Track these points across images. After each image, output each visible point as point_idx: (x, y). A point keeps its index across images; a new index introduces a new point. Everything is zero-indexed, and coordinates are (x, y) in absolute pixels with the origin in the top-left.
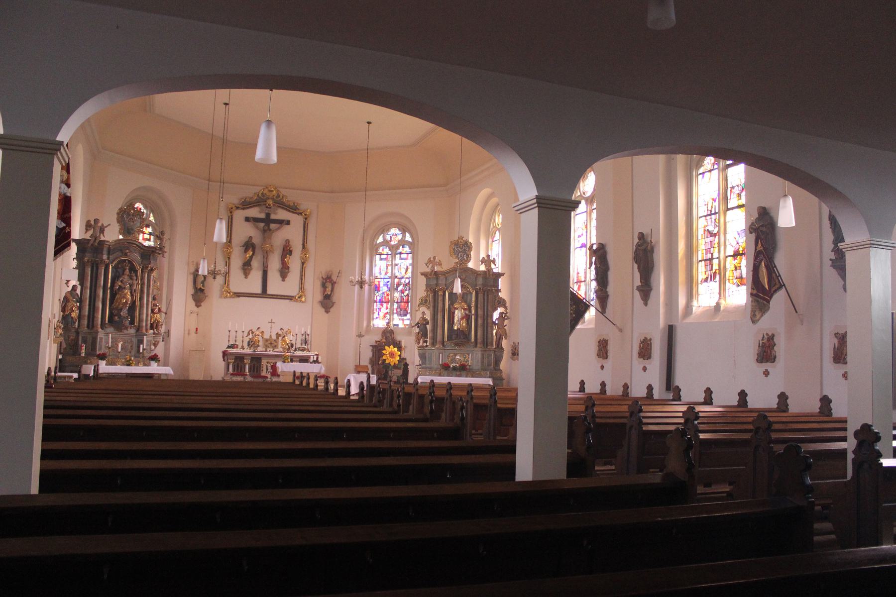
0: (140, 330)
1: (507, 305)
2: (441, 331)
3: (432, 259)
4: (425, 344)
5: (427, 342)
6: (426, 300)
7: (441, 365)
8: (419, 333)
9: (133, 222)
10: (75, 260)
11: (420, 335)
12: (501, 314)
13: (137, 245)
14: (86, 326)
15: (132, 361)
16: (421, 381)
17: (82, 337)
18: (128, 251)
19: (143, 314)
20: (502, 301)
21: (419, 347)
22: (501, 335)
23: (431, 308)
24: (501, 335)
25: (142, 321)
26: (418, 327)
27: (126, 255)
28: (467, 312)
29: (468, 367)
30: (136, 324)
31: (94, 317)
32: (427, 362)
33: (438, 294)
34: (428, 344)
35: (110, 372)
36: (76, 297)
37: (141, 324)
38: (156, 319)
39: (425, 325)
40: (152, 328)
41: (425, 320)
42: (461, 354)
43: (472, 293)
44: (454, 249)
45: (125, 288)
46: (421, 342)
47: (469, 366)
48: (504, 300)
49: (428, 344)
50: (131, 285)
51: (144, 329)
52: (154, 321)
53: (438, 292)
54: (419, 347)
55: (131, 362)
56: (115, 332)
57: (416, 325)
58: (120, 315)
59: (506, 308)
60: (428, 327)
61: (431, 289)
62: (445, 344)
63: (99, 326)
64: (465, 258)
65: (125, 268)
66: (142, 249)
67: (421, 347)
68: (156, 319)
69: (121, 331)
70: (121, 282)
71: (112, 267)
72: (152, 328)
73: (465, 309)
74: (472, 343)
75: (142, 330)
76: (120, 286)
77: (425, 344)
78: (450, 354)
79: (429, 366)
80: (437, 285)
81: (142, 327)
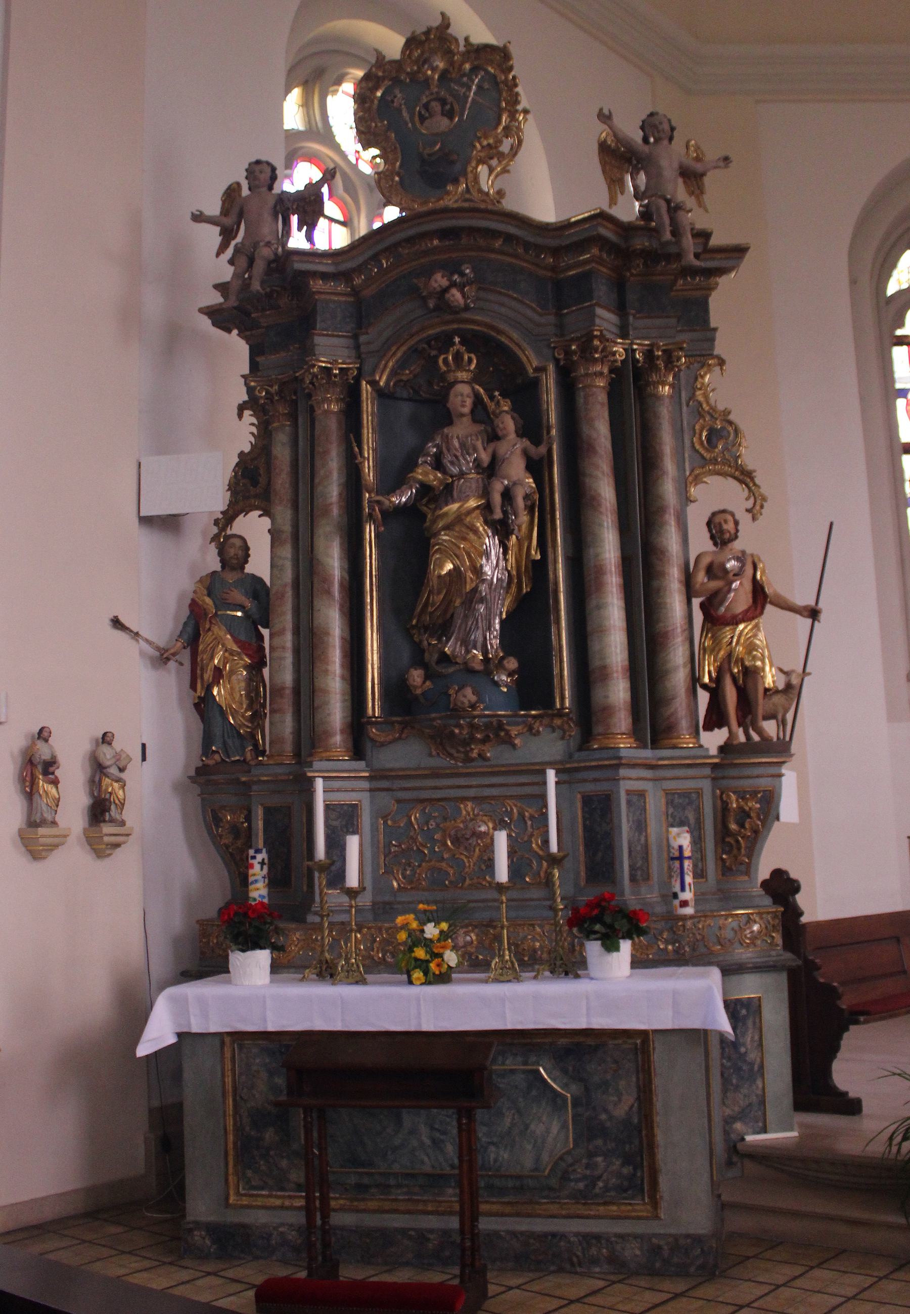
0: (598, 729)
9: (450, 115)
10: (247, 413)
13: (509, 238)
14: (288, 747)
15: (428, 944)
17: (268, 811)
18: (439, 280)
19: (602, 631)
25: (604, 674)
27: (443, 305)
30: (566, 697)
31: (313, 691)
35: (271, 1028)
36: (238, 596)
37: (598, 695)
38: (730, 655)
40: (716, 718)
45: (448, 492)
50: (491, 470)
51: (622, 721)
52: (719, 670)
55: (420, 953)
56: (440, 762)
58: (445, 659)
63: (338, 739)
65: (451, 377)
66: (539, 248)
68: (730, 655)
69: (468, 760)
70: (438, 464)
71: (381, 394)
72: (716, 718)
75: (607, 734)
76: (425, 489)
81: (608, 710)
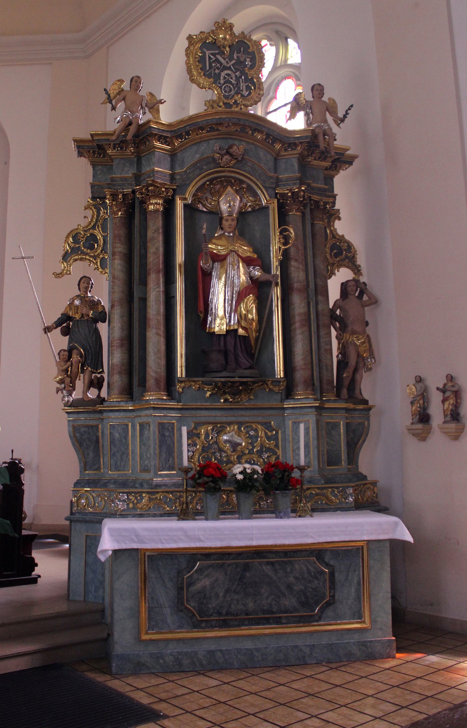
1: (361, 260)
2: (162, 340)
3: (126, 86)
4: (92, 394)
5: (100, 387)
6: (93, 238)
7: (186, 471)
8: (70, 351)
11: (75, 358)
12: (344, 286)
16: (117, 547)
20: (345, 246)
21: (67, 404)
22: (359, 355)
23: (118, 263)
24: (359, 355)
26: (65, 332)
28: (257, 273)
29: (296, 474)
32: (105, 459)
33: (144, 212)
34: (104, 393)
39: (95, 321)
41: (94, 304)
42: (240, 424)
43: (267, 208)
44: (202, 60)
46: (80, 384)
47: (302, 469)
48: (350, 246)
49: (104, 393)
53: (143, 202)
54: (67, 404)
57: (58, 323)
59: (356, 269)
60: (103, 328)
61: (114, 196)
62: (179, 387)
64: (243, 86)
67: (75, 404)
73: (248, 262)
74: (278, 382)
77: (92, 394)
78: (198, 425)
79: (112, 474)
80: (137, 178)
